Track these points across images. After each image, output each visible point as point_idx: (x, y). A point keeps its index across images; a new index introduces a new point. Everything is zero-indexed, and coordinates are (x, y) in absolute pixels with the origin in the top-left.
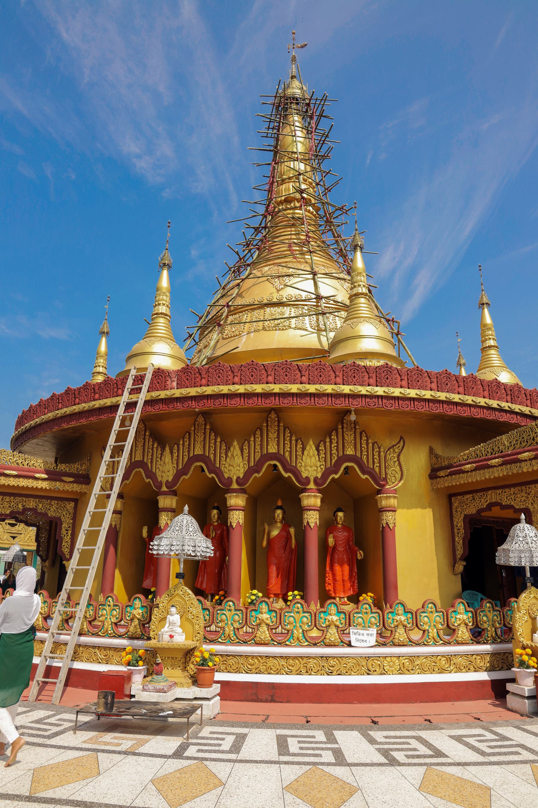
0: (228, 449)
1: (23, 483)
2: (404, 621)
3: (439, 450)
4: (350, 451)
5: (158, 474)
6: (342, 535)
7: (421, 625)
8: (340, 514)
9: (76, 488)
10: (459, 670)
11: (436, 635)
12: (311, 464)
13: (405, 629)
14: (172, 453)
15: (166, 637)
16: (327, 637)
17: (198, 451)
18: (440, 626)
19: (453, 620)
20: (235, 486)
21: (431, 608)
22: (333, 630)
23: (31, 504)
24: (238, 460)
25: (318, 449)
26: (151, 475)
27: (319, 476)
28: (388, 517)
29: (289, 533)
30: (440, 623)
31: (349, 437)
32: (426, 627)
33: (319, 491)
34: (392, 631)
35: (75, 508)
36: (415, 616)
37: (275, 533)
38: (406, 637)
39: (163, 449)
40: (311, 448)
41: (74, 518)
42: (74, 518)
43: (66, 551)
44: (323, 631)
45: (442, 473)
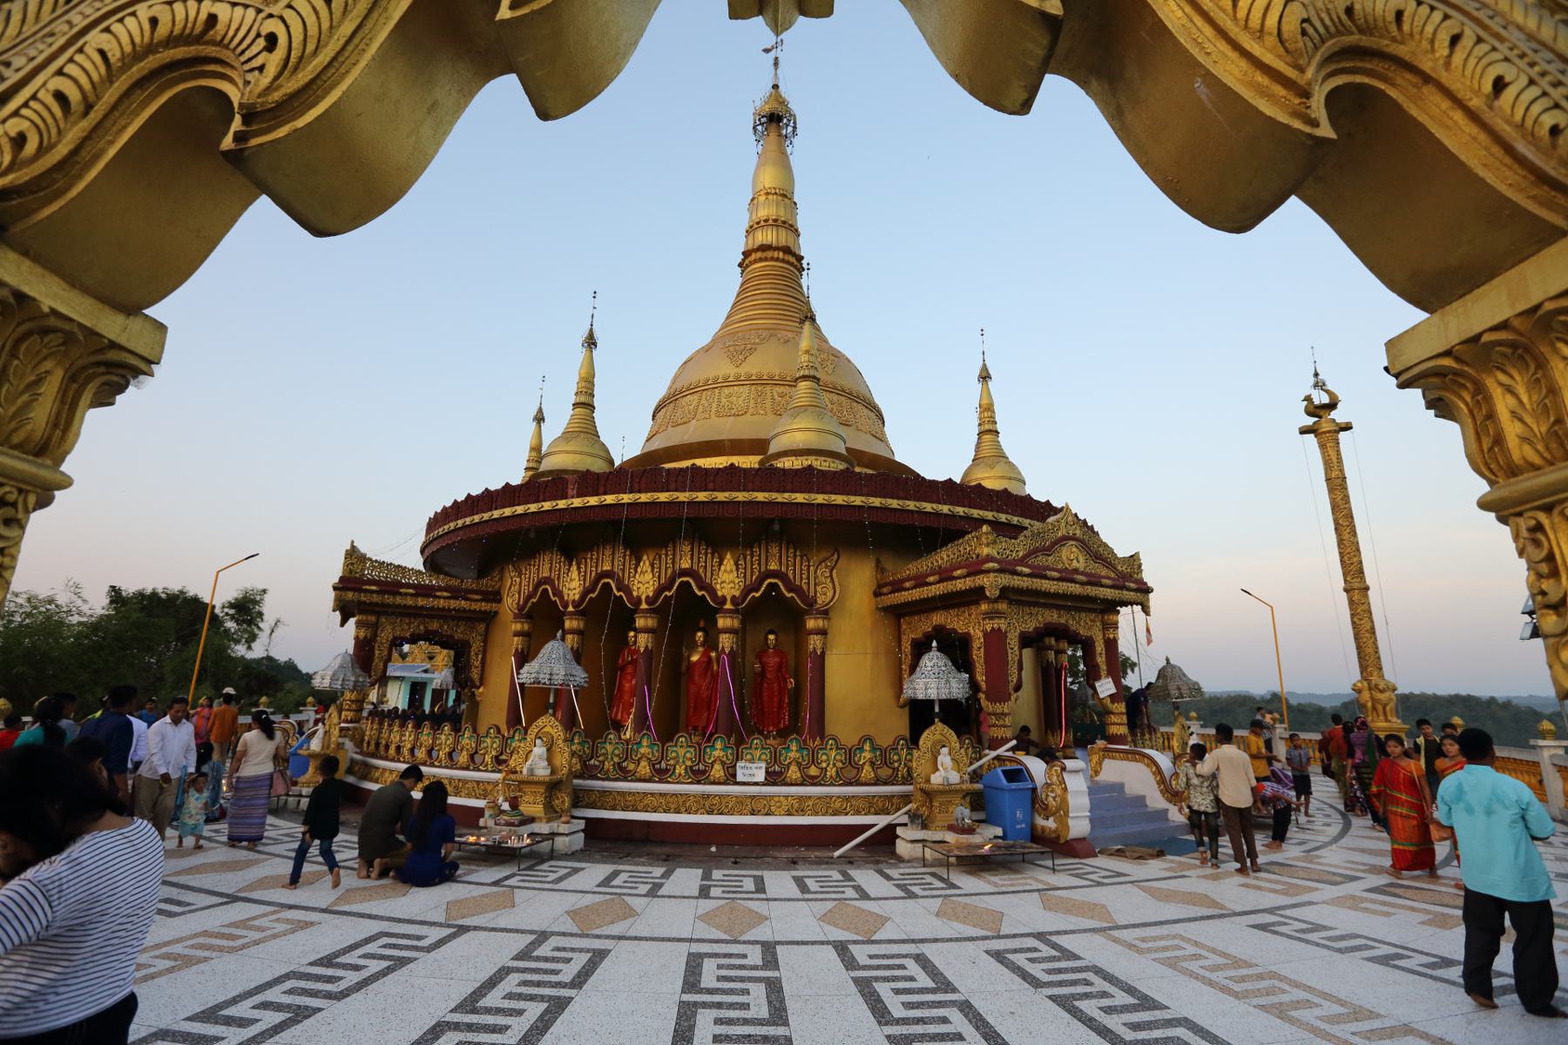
0: (637, 565)
1: (421, 602)
3: (888, 564)
4: (773, 566)
5: (565, 591)
6: (772, 661)
8: (771, 637)
9: (485, 606)
10: (858, 813)
12: (728, 579)
14: (579, 568)
15: (525, 771)
17: (607, 567)
20: (644, 606)
22: (717, 767)
23: (435, 625)
24: (649, 576)
25: (737, 564)
26: (558, 593)
27: (737, 594)
28: (815, 642)
29: (710, 658)
31: (775, 550)
33: (736, 611)
35: (487, 629)
36: (850, 754)
37: (695, 658)
39: (570, 565)
40: (729, 562)
41: (485, 641)
42: (485, 641)
43: (475, 675)
45: (885, 590)
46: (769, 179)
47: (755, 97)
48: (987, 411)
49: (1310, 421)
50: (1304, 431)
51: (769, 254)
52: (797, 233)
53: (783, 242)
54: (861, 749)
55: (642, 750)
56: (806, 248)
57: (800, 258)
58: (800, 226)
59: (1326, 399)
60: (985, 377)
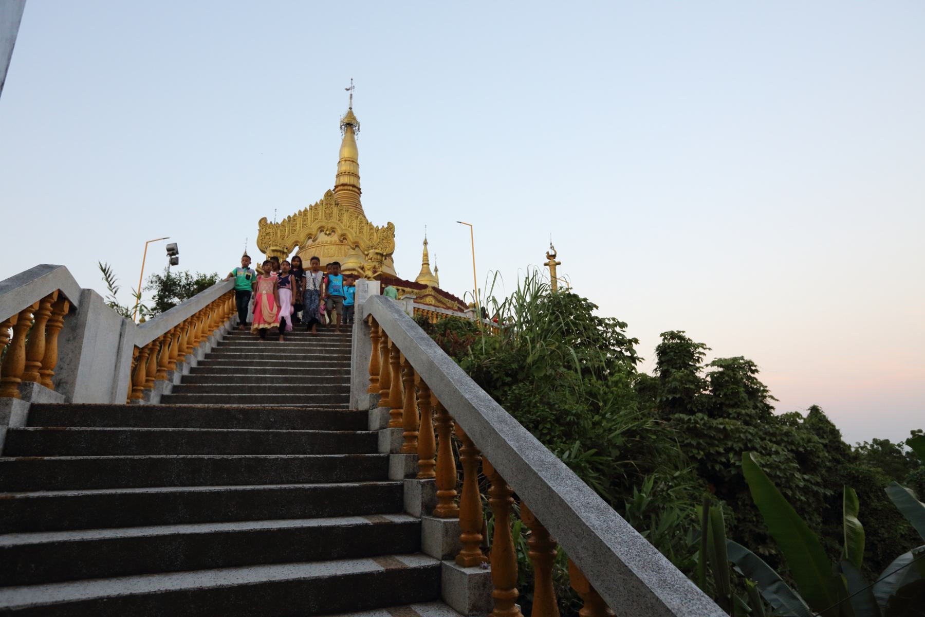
46: (347, 153)
47: (342, 113)
48: (426, 255)
49: (547, 261)
50: (546, 265)
51: (346, 187)
52: (359, 178)
53: (352, 183)
56: (363, 184)
57: (359, 189)
58: (360, 175)
59: (553, 253)
60: (426, 243)
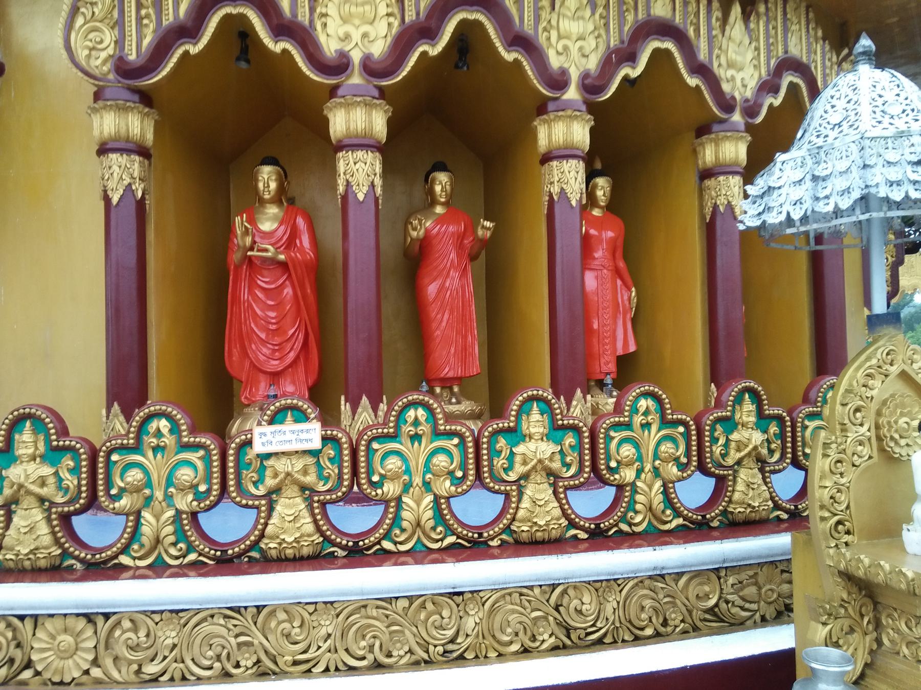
2: (551, 459)
7: (609, 468)
11: (658, 500)
13: (554, 486)
16: (270, 530)
18: (675, 470)
19: (718, 450)
21: (647, 412)
30: (677, 459)
32: (628, 475)
34: (507, 495)
38: (557, 512)
44: (257, 508)
54: (729, 423)
55: (15, 473)
